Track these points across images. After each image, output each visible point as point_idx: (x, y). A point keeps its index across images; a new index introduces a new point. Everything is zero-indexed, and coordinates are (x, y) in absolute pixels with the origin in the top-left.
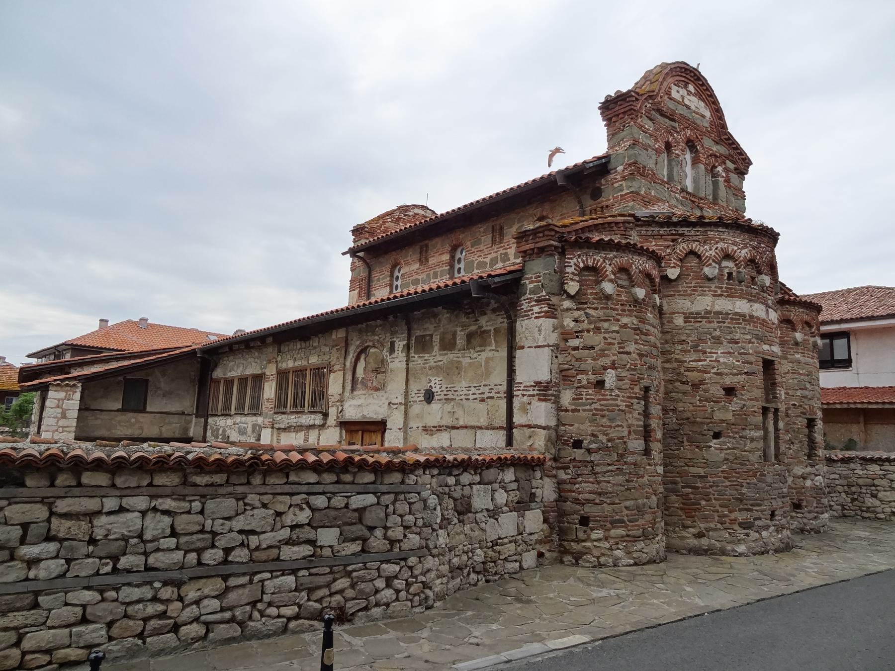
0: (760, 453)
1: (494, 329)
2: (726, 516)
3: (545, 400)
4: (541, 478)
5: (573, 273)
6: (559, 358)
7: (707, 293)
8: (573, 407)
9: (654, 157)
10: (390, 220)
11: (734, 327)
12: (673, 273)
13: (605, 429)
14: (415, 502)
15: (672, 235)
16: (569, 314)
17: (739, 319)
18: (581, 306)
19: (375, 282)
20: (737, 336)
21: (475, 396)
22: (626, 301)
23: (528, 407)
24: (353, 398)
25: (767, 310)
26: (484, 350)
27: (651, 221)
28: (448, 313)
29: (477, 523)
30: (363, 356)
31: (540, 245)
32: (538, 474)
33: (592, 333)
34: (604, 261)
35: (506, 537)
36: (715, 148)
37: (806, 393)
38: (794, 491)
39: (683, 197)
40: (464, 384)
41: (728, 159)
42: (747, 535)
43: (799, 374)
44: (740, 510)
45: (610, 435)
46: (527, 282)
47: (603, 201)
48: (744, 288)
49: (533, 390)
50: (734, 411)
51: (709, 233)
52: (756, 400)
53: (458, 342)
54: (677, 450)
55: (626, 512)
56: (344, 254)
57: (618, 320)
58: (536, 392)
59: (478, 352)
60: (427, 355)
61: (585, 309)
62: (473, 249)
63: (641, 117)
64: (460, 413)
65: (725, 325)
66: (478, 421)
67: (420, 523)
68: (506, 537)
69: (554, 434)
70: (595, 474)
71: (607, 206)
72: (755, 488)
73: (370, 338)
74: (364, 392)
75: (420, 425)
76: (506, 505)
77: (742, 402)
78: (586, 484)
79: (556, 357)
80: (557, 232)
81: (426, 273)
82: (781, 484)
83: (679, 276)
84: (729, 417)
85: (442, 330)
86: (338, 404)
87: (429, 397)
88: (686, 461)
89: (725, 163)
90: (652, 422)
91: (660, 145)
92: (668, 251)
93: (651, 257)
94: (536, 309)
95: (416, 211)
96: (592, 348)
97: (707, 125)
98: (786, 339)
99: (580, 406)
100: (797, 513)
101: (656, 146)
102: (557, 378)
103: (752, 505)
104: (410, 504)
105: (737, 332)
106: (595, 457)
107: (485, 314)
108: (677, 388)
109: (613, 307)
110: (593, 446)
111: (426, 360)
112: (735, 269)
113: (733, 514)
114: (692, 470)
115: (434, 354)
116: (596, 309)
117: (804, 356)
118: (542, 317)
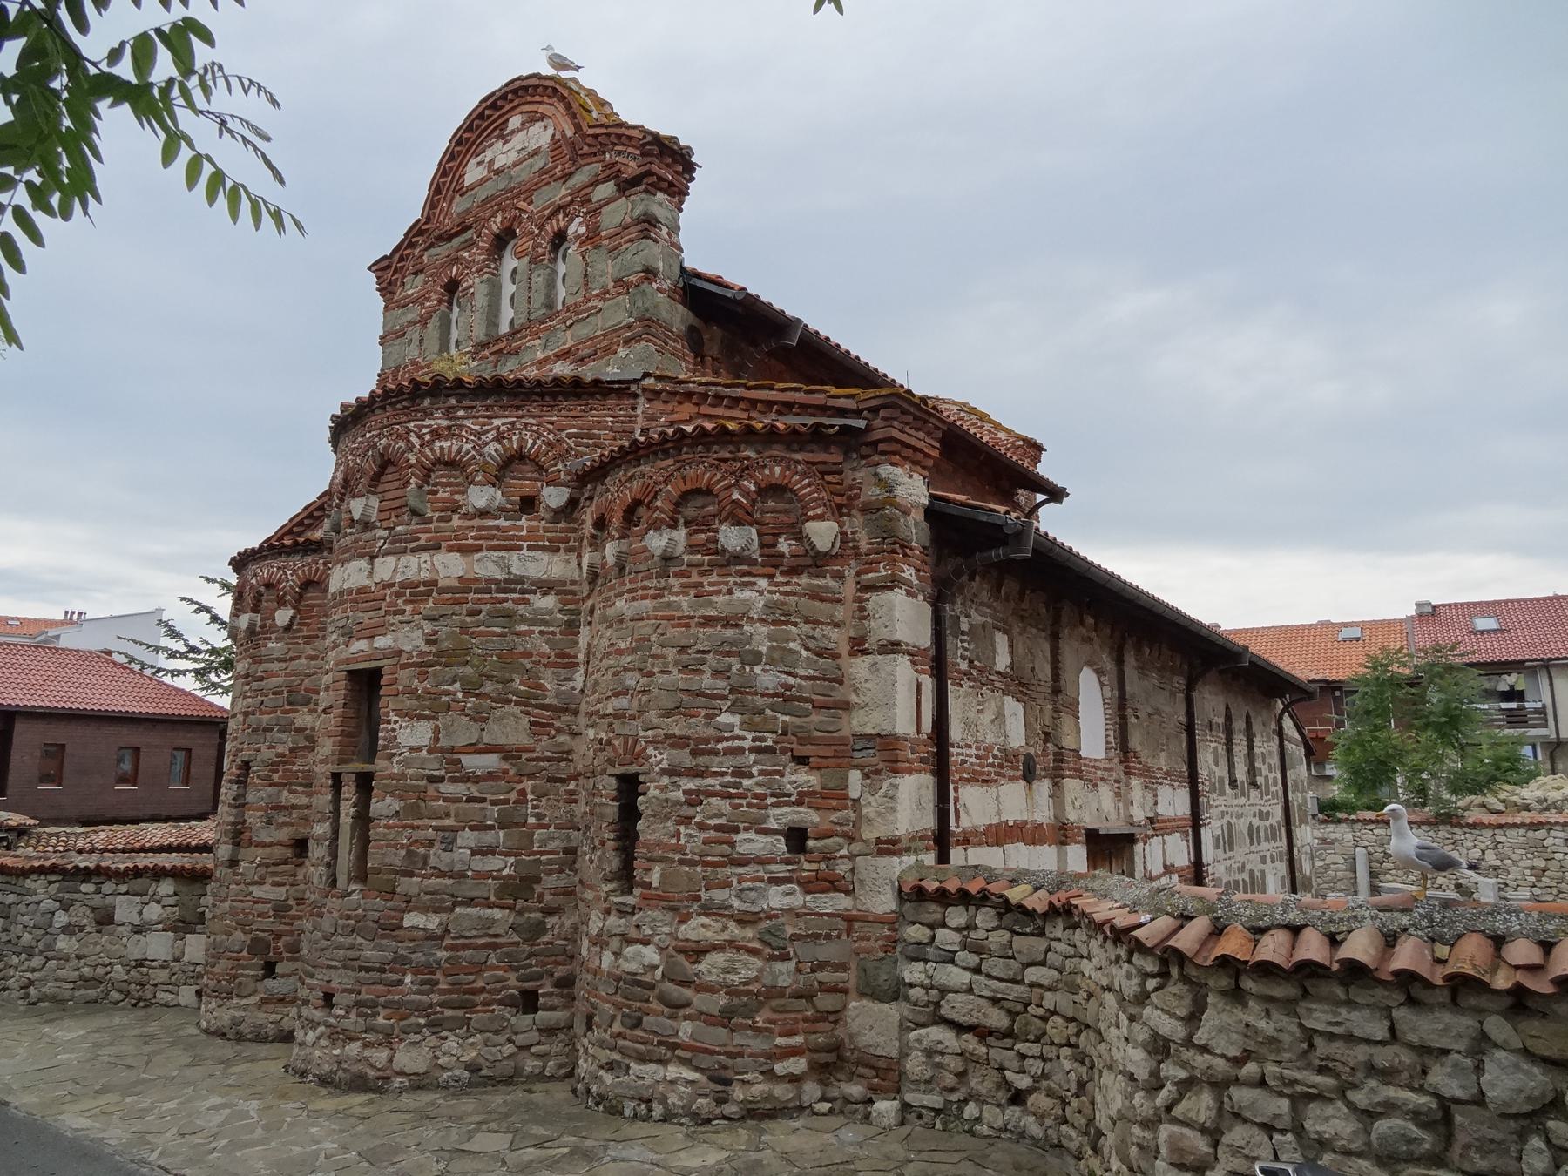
82: (360, 940)
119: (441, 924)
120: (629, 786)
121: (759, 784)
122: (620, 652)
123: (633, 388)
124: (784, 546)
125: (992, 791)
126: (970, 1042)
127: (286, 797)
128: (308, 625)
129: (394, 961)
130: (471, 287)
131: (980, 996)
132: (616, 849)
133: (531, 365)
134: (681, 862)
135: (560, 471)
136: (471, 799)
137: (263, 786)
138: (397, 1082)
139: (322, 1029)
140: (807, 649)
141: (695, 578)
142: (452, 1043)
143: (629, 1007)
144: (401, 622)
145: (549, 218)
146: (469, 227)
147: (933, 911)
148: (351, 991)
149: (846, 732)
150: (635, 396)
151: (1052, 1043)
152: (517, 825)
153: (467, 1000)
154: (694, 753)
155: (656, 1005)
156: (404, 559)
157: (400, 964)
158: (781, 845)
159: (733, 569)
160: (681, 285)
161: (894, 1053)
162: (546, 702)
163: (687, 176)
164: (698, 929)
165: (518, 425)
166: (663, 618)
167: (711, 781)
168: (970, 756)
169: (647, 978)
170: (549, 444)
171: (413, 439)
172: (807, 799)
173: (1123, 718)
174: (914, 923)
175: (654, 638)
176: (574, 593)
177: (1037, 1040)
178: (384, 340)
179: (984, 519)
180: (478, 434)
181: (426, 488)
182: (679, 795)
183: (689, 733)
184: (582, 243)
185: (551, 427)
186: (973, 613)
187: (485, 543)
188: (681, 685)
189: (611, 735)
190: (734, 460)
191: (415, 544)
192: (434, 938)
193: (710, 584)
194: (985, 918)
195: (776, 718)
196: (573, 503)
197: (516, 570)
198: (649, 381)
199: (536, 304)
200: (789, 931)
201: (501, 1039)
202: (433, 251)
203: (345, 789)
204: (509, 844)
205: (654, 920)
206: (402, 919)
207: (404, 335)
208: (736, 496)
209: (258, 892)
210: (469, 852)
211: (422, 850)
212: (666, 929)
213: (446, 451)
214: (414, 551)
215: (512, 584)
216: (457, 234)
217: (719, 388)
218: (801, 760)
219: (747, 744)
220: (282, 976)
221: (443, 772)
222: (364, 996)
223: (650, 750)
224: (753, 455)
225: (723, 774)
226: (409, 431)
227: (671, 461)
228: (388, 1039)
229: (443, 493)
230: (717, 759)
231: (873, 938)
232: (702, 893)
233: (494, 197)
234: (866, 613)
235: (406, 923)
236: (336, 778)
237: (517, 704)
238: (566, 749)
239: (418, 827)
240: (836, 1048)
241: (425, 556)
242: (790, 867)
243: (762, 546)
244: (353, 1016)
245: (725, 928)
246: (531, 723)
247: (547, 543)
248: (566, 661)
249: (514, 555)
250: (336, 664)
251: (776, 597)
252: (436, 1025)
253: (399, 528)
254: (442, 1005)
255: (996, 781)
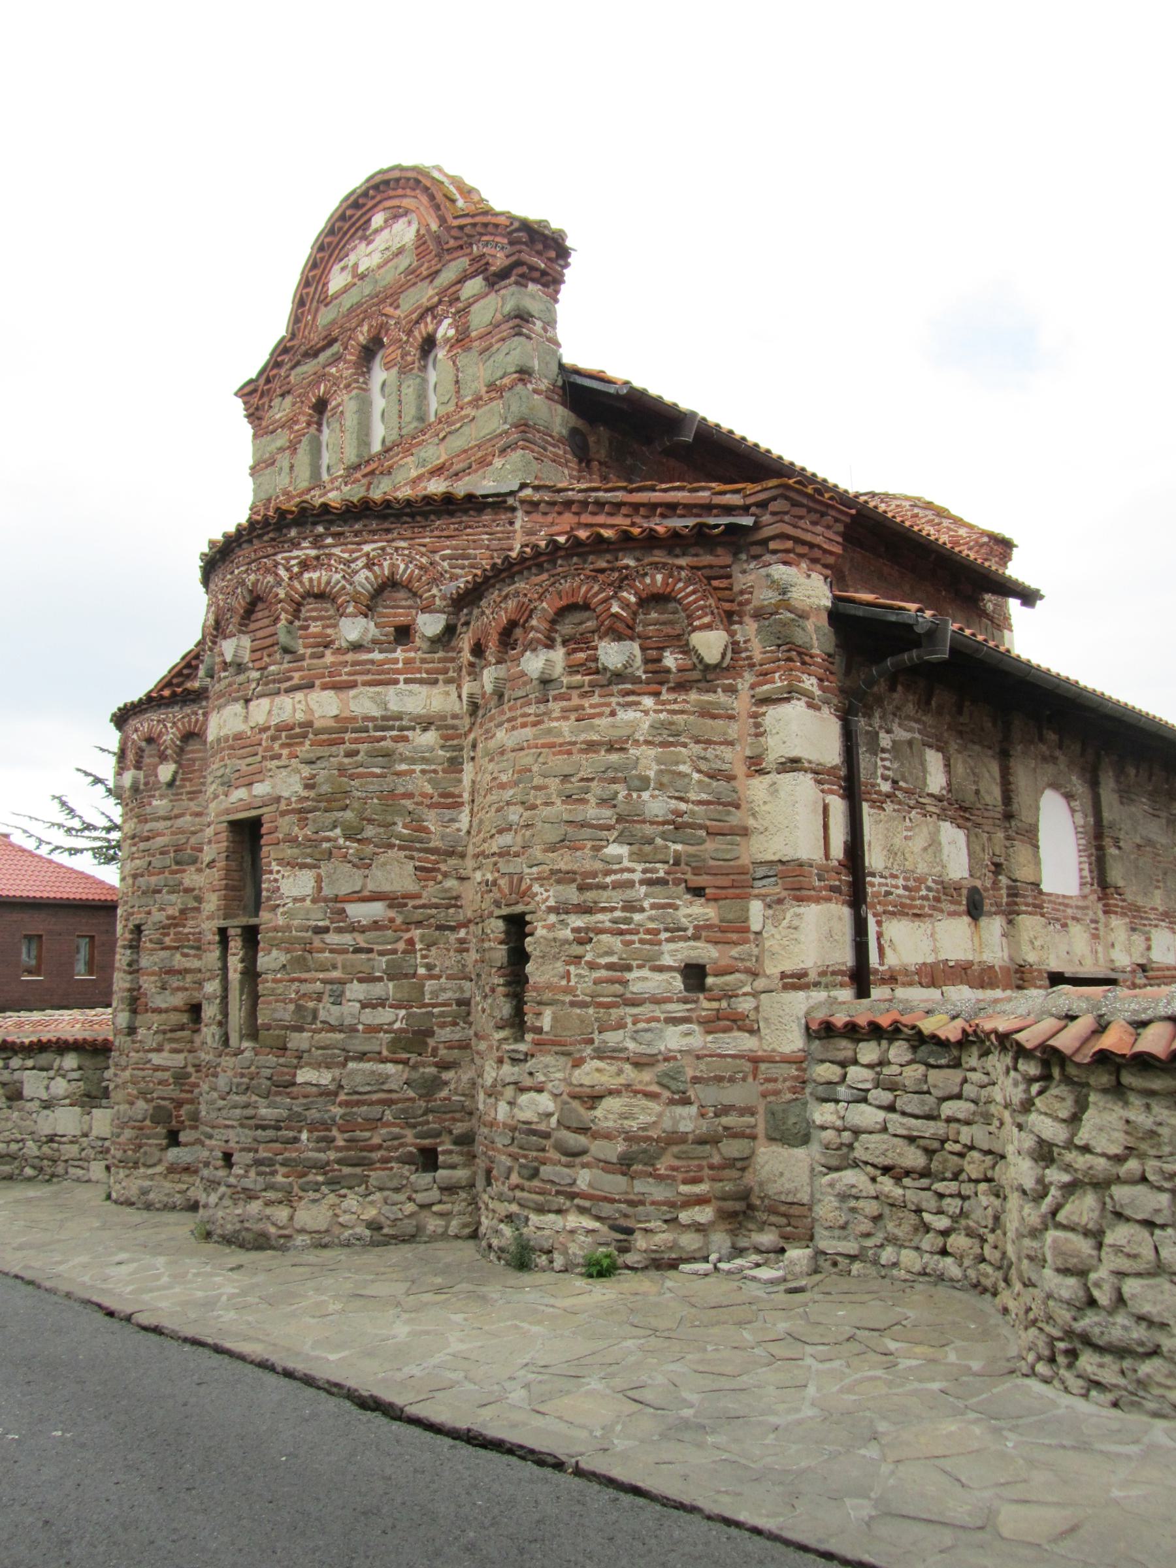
82: (254, 1098)
119: (333, 1080)
120: (517, 926)
121: (651, 919)
122: (502, 786)
123: (510, 501)
124: (670, 660)
125: (925, 926)
126: (887, 1184)
127: (178, 961)
128: (190, 780)
129: (289, 1118)
130: (339, 405)
131: (895, 1135)
132: (506, 995)
133: (405, 484)
134: (573, 1004)
135: (434, 596)
136: (358, 950)
137: (155, 950)
138: (300, 1240)
139: (223, 1189)
140: (699, 771)
141: (576, 701)
142: (352, 1201)
143: (525, 1157)
144: (278, 767)
145: (417, 322)
146: (335, 340)
147: (844, 1048)
148: (249, 1150)
149: (745, 860)
150: (513, 509)
151: (970, 1180)
152: (406, 976)
153: (365, 1158)
154: (581, 888)
155: (553, 1154)
156: (278, 700)
157: (295, 1120)
158: (678, 983)
159: (615, 688)
160: (560, 383)
161: (806, 1199)
162: (432, 845)
163: (562, 262)
164: (593, 1073)
165: (389, 550)
166: (544, 746)
167: (600, 917)
168: (897, 887)
169: (542, 1127)
170: (421, 568)
171: (282, 572)
172: (704, 934)
173: (1100, 848)
174: (823, 1061)
175: (535, 768)
176: (454, 727)
177: (955, 1177)
178: (255, 471)
179: (893, 618)
180: (347, 563)
181: (297, 623)
182: (567, 934)
183: (575, 867)
184: (452, 346)
185: (423, 549)
186: (895, 728)
187: (359, 678)
188: (565, 817)
189: (496, 875)
190: (612, 570)
191: (288, 684)
192: (329, 1094)
193: (592, 706)
194: (898, 1052)
195: (667, 847)
196: (450, 631)
197: (394, 707)
198: (528, 492)
199: (407, 418)
200: (690, 1073)
201: (401, 1197)
202: (299, 369)
203: (232, 944)
204: (399, 996)
205: (547, 1066)
206: (295, 1075)
207: (273, 464)
208: (615, 609)
209: (157, 1059)
210: (358, 1005)
211: (311, 1004)
212: (559, 1075)
213: (315, 583)
214: (288, 691)
215: (388, 721)
216: (323, 349)
217: (601, 494)
218: (698, 892)
219: (637, 876)
220: (186, 1145)
221: (327, 923)
222: (263, 1154)
223: (536, 888)
224: (632, 563)
225: (613, 909)
226: (276, 564)
227: (545, 576)
228: (288, 1199)
229: (315, 628)
230: (605, 894)
231: (781, 1079)
232: (596, 1036)
233: (359, 304)
234: (762, 729)
235: (300, 1079)
236: (223, 932)
237: (401, 848)
238: (454, 894)
239: (305, 981)
240: (744, 1196)
241: (299, 695)
242: (689, 1006)
243: (646, 661)
244: (252, 1173)
245: (620, 1072)
246: (416, 868)
247: (424, 675)
248: (450, 802)
249: (391, 689)
250: (217, 816)
251: (663, 716)
252: (334, 1183)
253: (272, 668)
254: (339, 1162)
255: (931, 916)
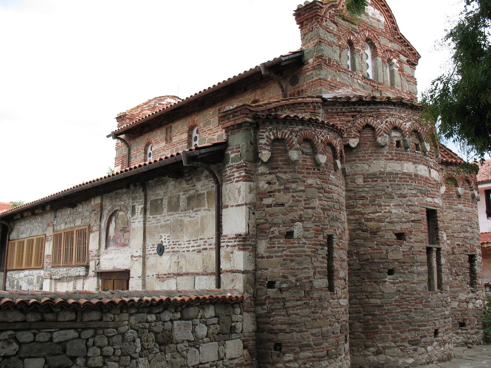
0: (426, 284)
1: (207, 192)
2: (399, 336)
3: (244, 249)
4: (240, 314)
5: (265, 144)
6: (256, 214)
7: (381, 157)
8: (268, 254)
9: (338, 51)
10: (147, 108)
11: (403, 185)
12: (353, 143)
13: (294, 271)
14: (113, 336)
15: (352, 112)
16: (263, 178)
17: (406, 178)
18: (273, 171)
19: (133, 159)
20: (405, 192)
21: (193, 249)
22: (311, 166)
23: (231, 255)
24: (107, 253)
25: (430, 170)
26: (200, 210)
27: (336, 101)
28: (173, 180)
29: (178, 352)
30: (114, 219)
31: (239, 122)
32: (238, 311)
33: (282, 193)
34: (291, 134)
35: (207, 363)
36: (390, 45)
37: (468, 235)
38: (459, 313)
39: (365, 83)
40: (186, 238)
41: (401, 53)
42: (415, 350)
43: (462, 220)
44: (409, 331)
45: (299, 276)
46: (230, 152)
47: (299, 87)
48: (409, 153)
49: (235, 241)
50: (403, 252)
51: (380, 110)
52: (421, 242)
53: (181, 204)
54: (360, 285)
55: (312, 338)
56: (108, 136)
57: (304, 181)
58: (236, 243)
59: (196, 211)
60: (159, 216)
61: (277, 173)
62: (205, 129)
63: (326, 21)
64: (183, 263)
65: (396, 183)
66: (196, 269)
67: (119, 352)
68: (207, 363)
69: (252, 278)
70: (286, 308)
71: (302, 91)
72: (421, 312)
73: (118, 203)
74: (114, 248)
75: (155, 274)
76: (207, 336)
77: (409, 244)
78: (279, 317)
79: (254, 214)
80: (251, 111)
81: (170, 150)
83: (358, 144)
84: (400, 257)
85: (169, 194)
86: (96, 258)
87: (161, 250)
88: (367, 294)
89: (399, 57)
90: (334, 264)
91: (343, 42)
92: (350, 125)
93: (332, 130)
94: (236, 174)
95: (169, 100)
96: (283, 205)
97: (383, 28)
98: (451, 193)
99: (273, 253)
100: (462, 329)
101: (340, 43)
102: (254, 231)
103: (418, 326)
104: (109, 338)
105: (405, 188)
106: (286, 295)
107: (200, 180)
108: (359, 236)
109: (300, 170)
110: (284, 286)
111: (158, 220)
112: (402, 138)
113: (404, 334)
114: (372, 301)
115: (164, 215)
116: (285, 173)
117: (465, 206)
118: (240, 181)
175: (473, 218)
